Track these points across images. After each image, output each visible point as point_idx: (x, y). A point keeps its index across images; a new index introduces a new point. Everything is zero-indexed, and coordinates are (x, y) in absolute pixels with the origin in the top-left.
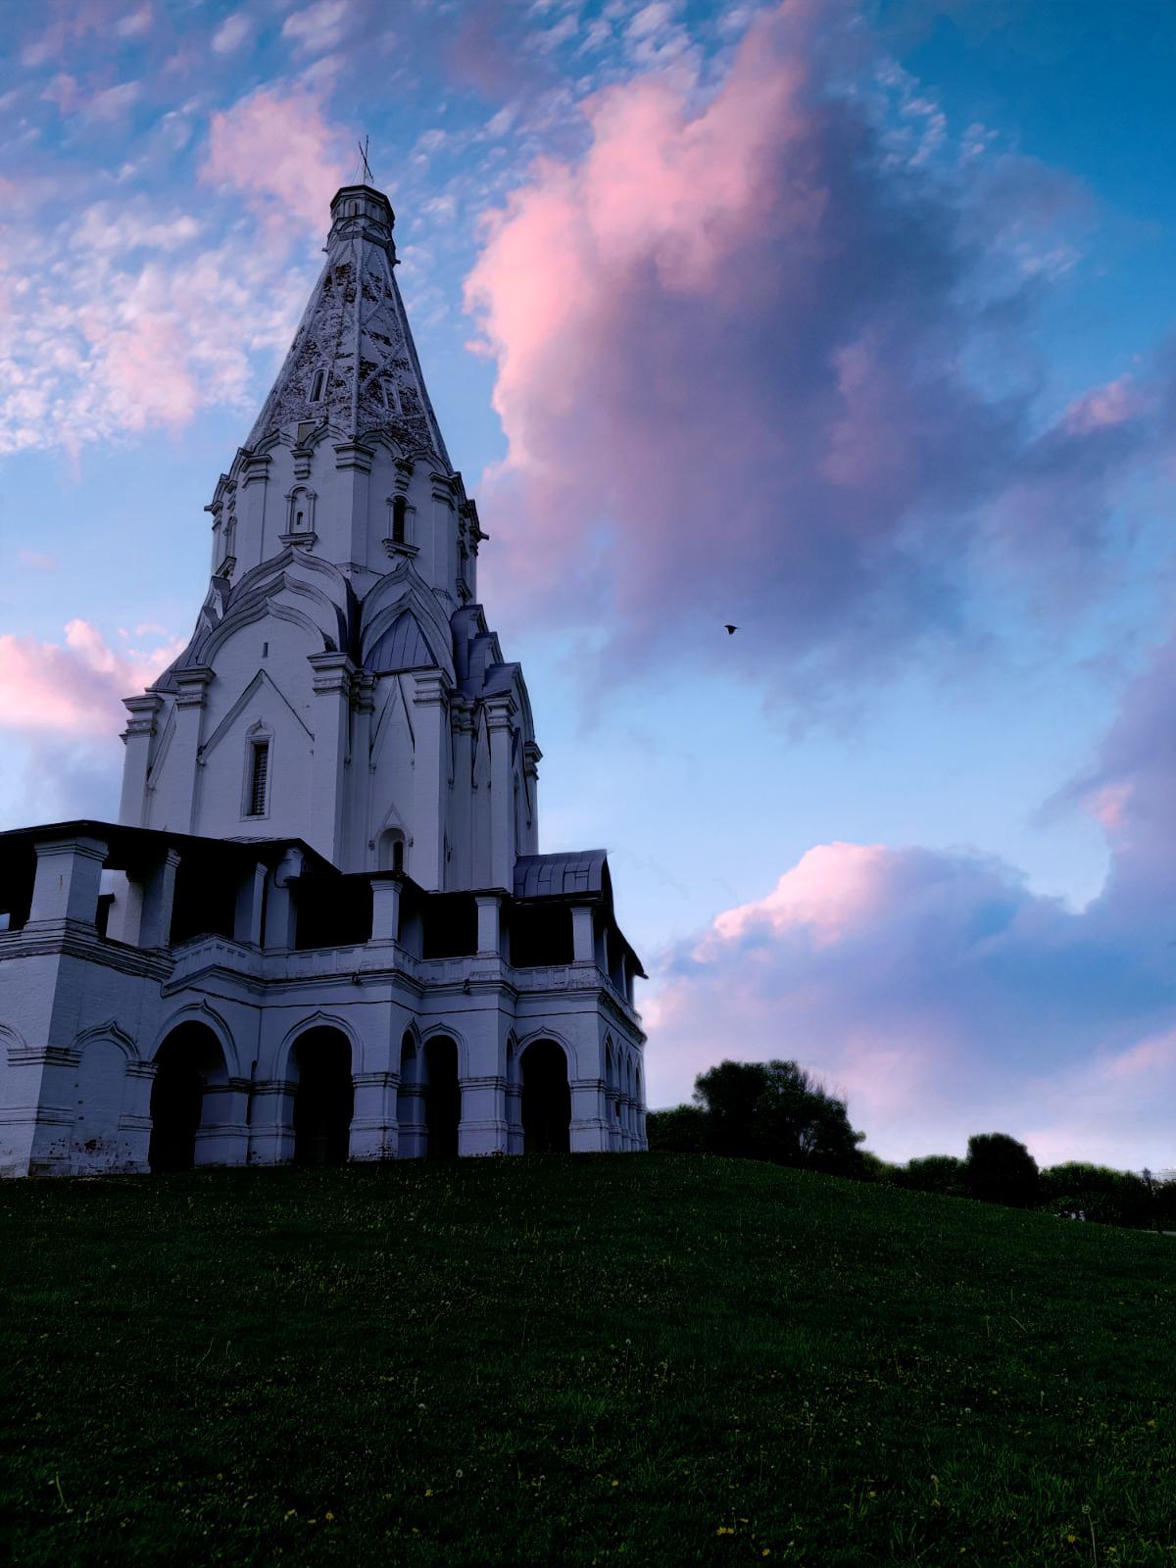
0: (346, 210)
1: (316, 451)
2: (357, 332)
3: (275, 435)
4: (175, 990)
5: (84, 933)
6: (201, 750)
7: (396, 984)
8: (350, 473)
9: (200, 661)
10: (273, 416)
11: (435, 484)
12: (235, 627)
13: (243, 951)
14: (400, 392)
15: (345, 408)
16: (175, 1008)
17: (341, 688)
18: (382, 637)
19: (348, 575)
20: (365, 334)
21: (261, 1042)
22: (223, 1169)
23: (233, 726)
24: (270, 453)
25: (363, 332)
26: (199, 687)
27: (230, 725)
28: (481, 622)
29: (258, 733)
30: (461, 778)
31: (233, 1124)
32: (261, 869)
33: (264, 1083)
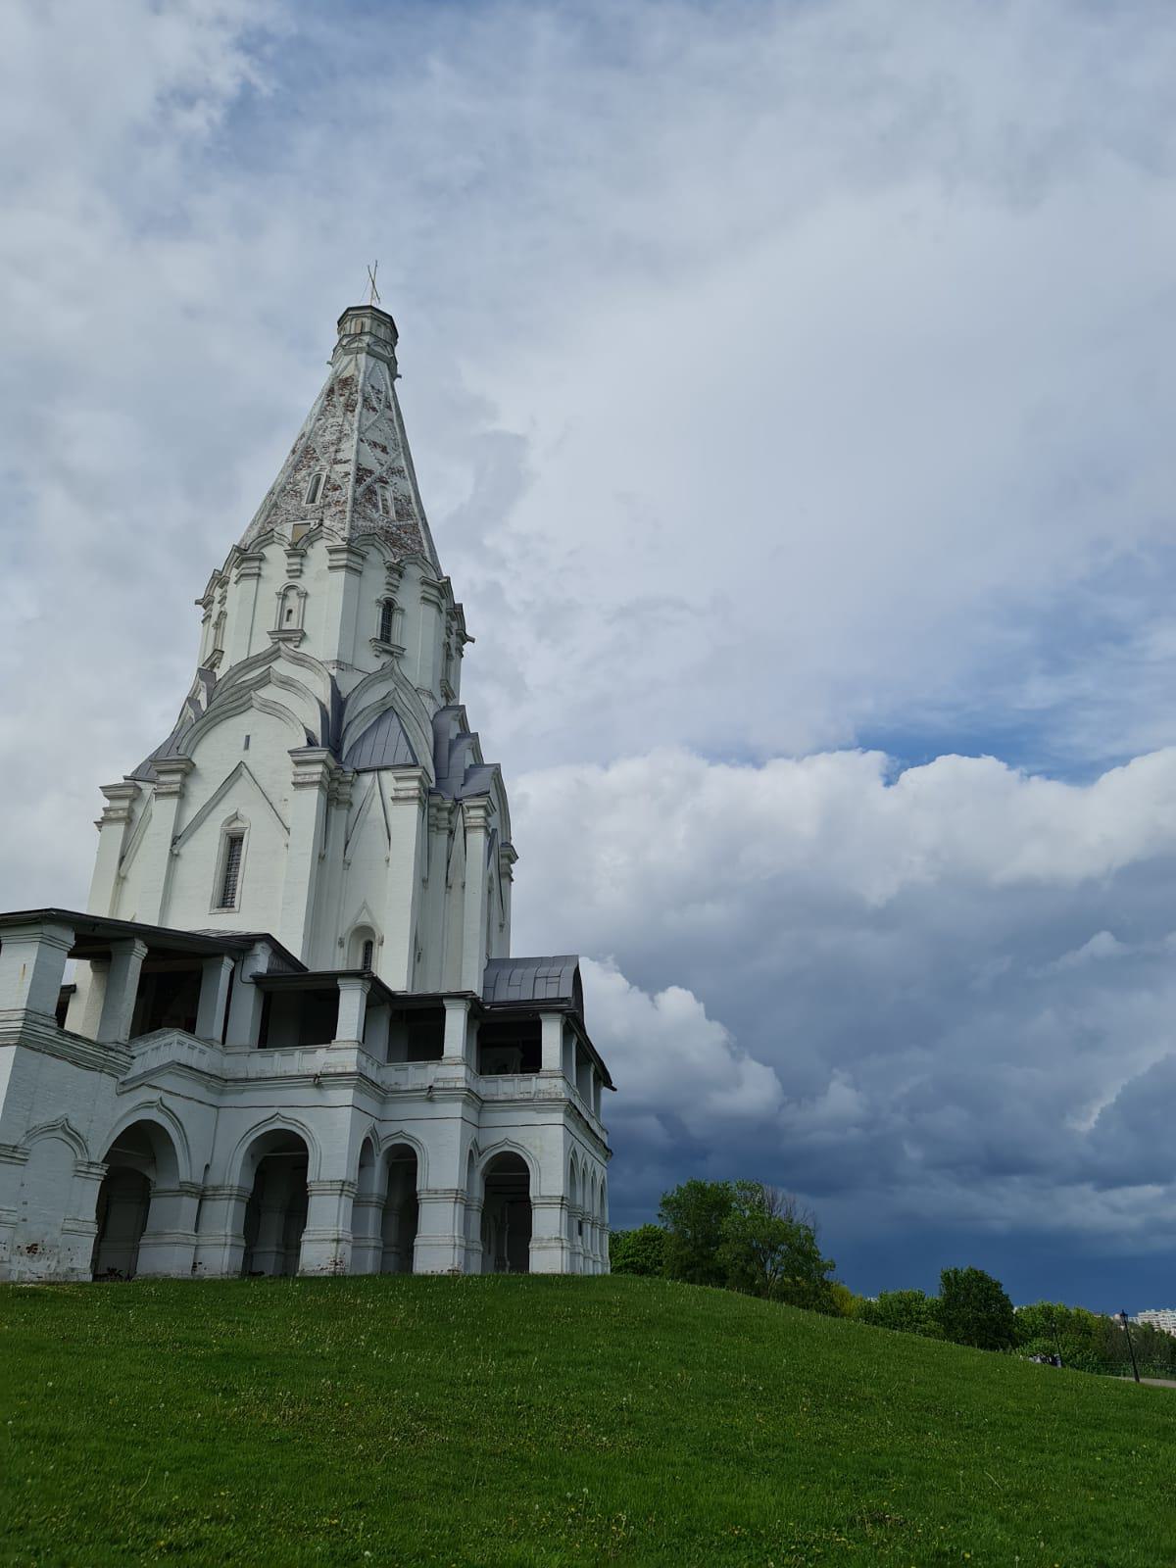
0: (352, 327)
1: (310, 552)
2: (354, 441)
3: (271, 534)
4: (132, 1087)
5: (42, 1025)
6: (175, 840)
7: (356, 1088)
8: (342, 574)
9: (181, 751)
10: (268, 516)
11: (425, 587)
12: (218, 720)
13: (203, 1047)
14: (395, 499)
15: (340, 512)
16: (132, 1105)
17: (320, 783)
18: (364, 734)
19: (334, 672)
20: (362, 441)
21: (215, 1147)
22: (167, 1281)
23: (209, 818)
24: (262, 551)
25: (362, 441)
26: (178, 777)
27: (208, 814)
28: (463, 721)
29: (234, 826)
30: (435, 876)
31: (180, 1231)
32: (228, 963)
33: (216, 1188)
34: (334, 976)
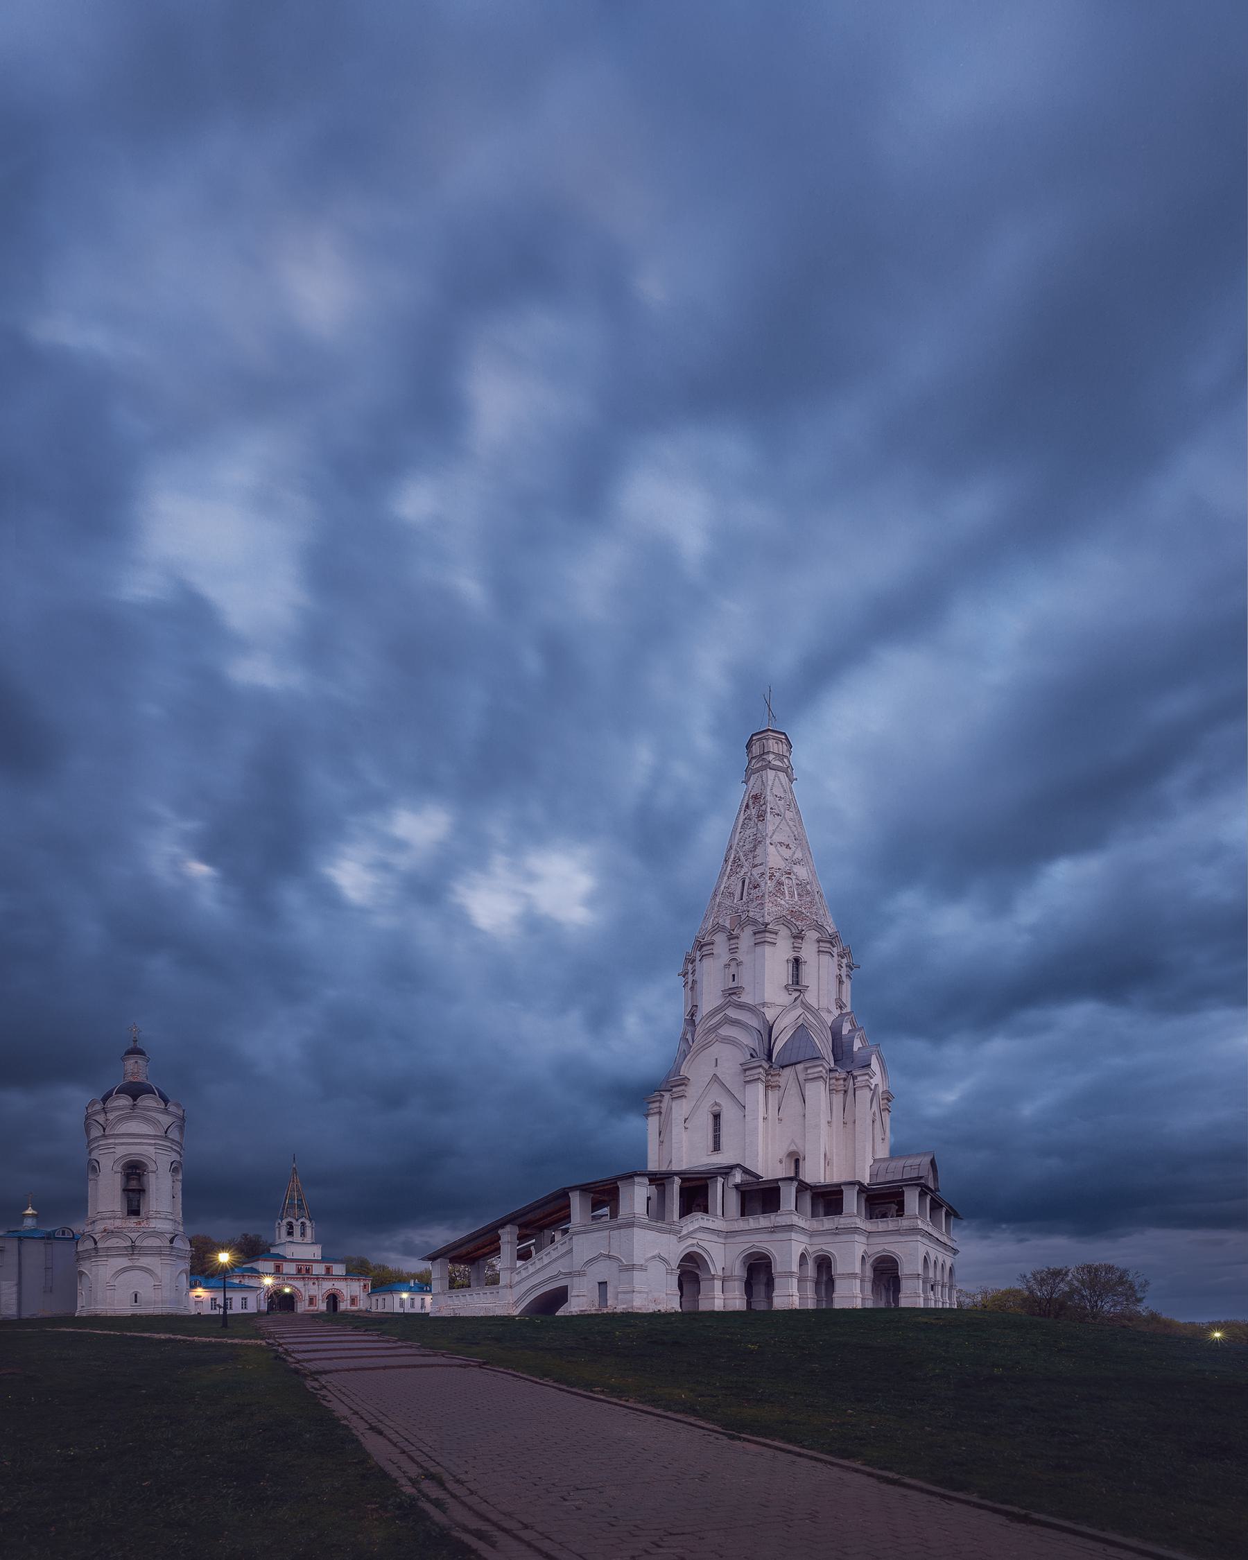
32: (720, 1180)
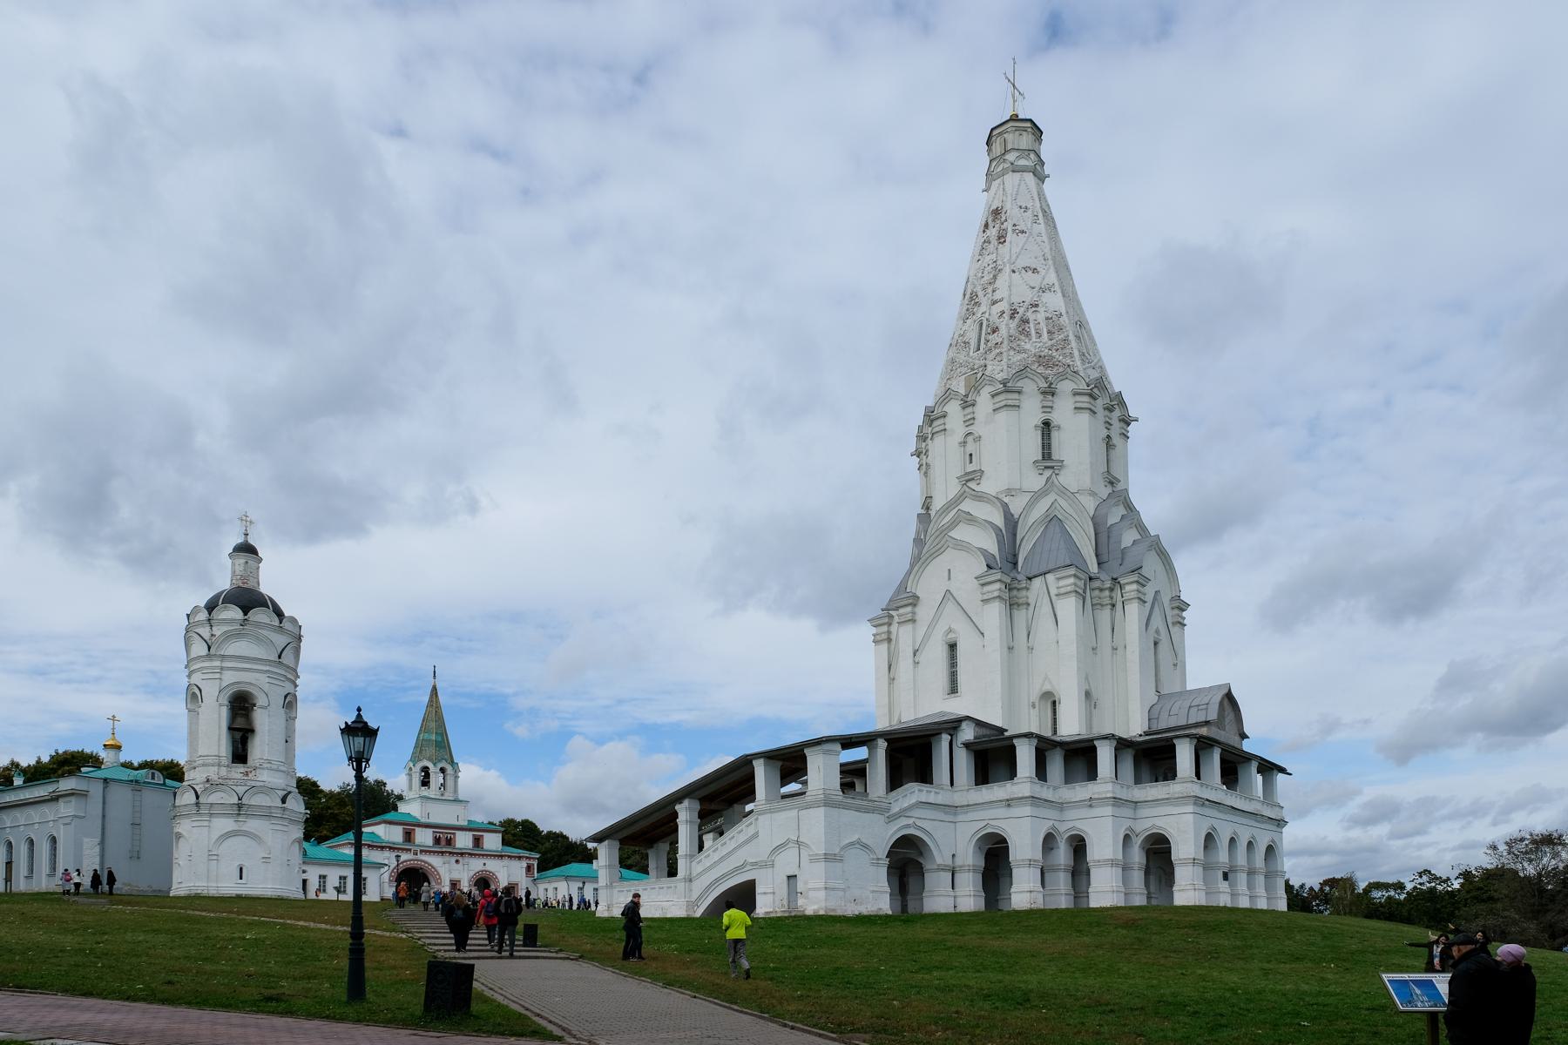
8: (1003, 415)
32: (945, 738)
34: (1012, 738)
